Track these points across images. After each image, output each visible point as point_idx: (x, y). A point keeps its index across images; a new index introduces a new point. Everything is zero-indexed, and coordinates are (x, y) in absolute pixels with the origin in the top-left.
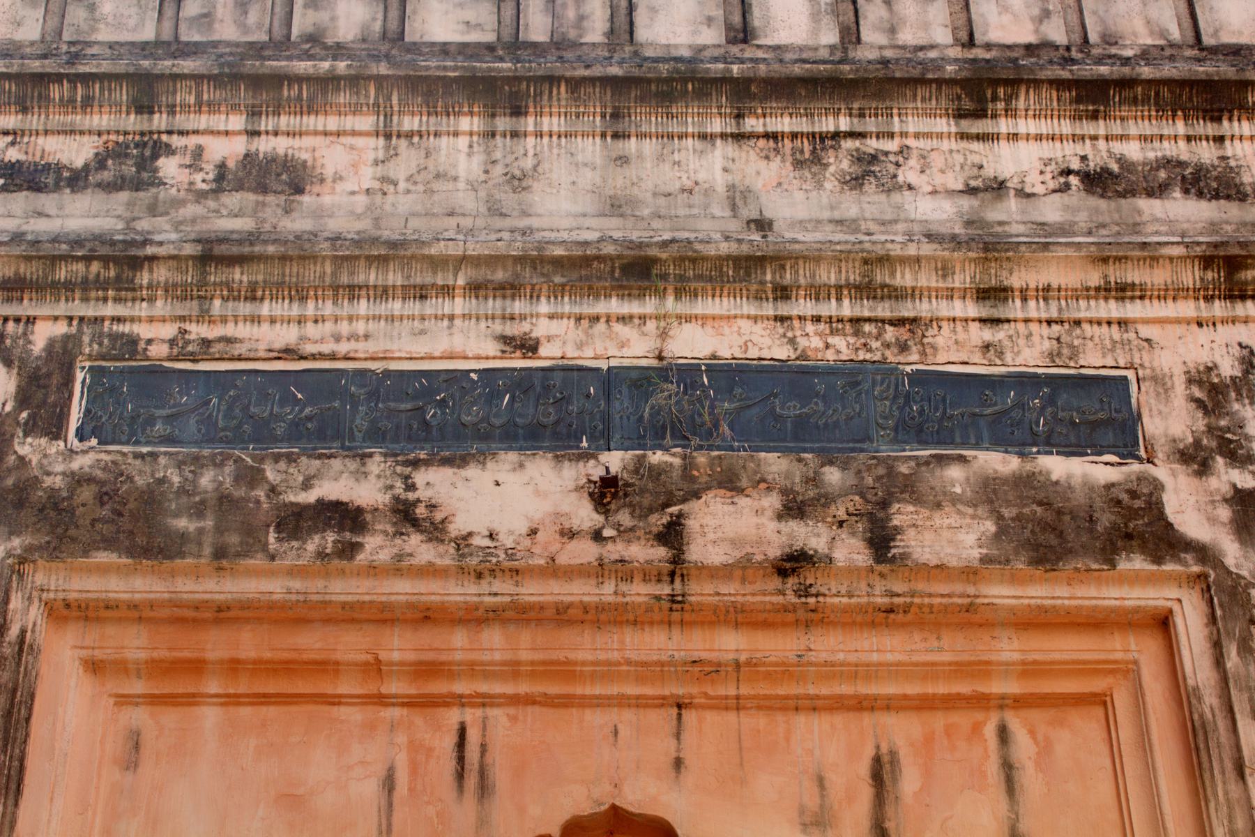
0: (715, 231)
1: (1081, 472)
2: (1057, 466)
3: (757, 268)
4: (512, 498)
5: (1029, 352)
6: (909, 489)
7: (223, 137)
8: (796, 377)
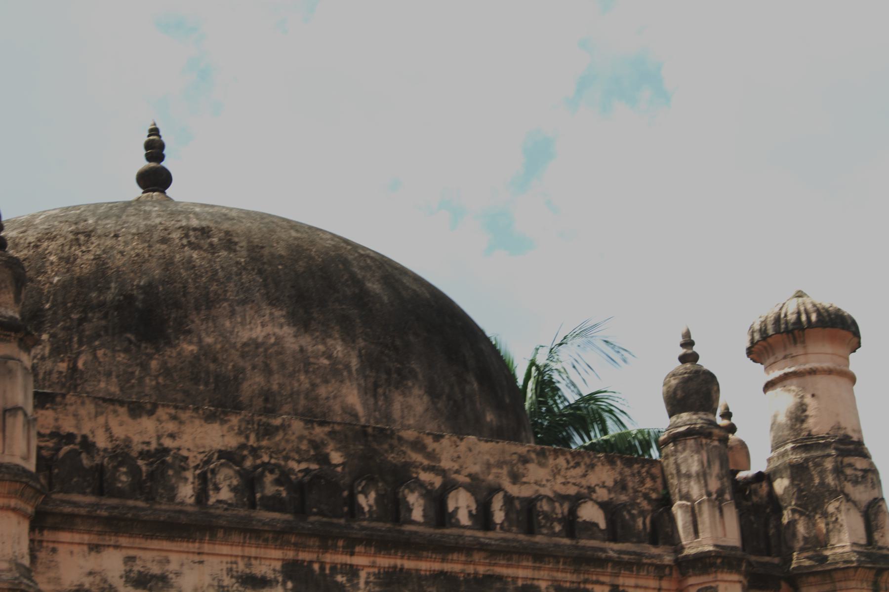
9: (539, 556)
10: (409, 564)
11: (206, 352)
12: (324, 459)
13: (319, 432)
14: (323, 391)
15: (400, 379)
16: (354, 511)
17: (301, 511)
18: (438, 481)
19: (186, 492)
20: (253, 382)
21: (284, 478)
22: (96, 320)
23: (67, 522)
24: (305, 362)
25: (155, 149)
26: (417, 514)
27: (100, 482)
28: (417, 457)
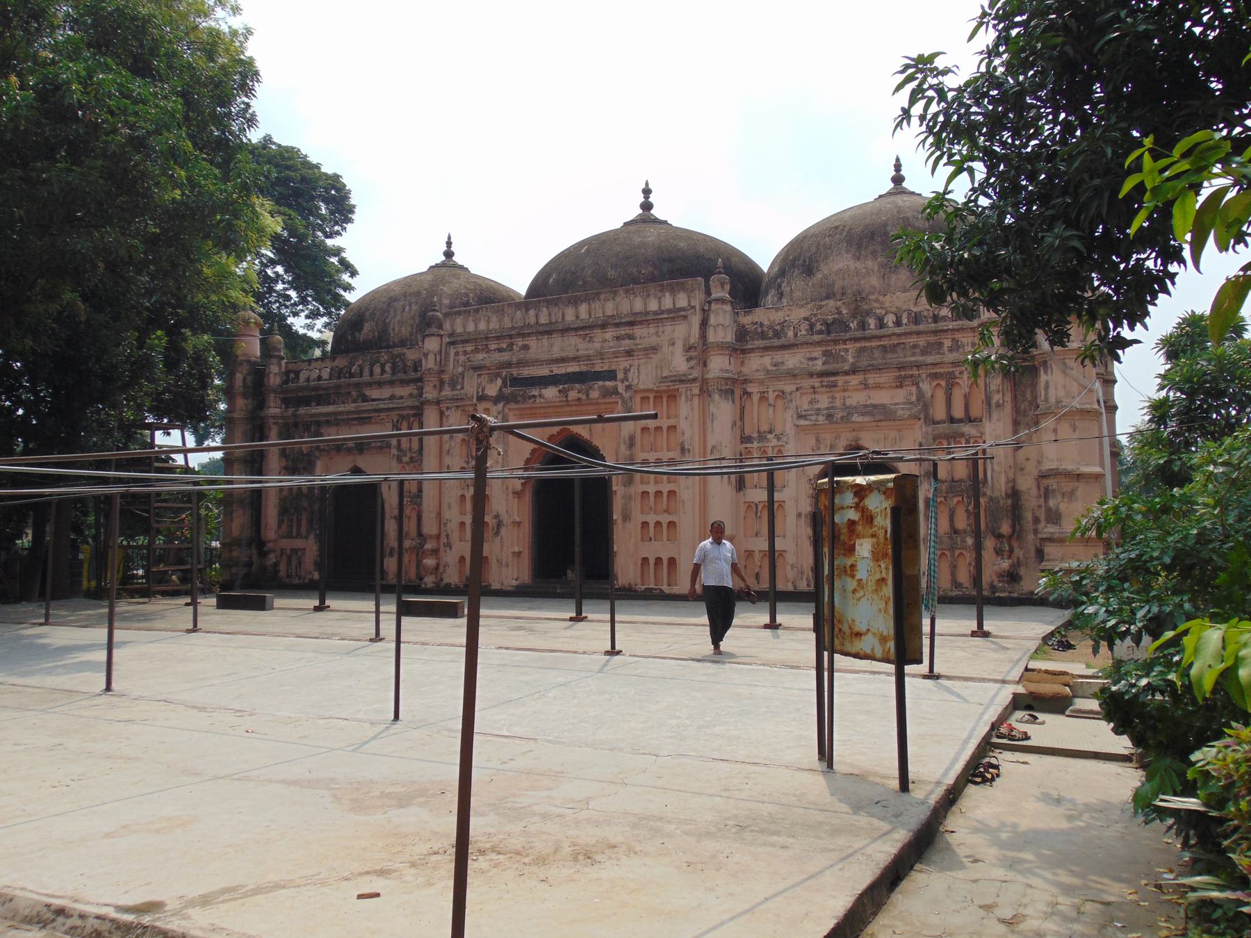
0: (571, 355)
2: (608, 383)
3: (575, 359)
4: (551, 392)
5: (606, 368)
6: (590, 388)
8: (580, 373)
9: (918, 333)
10: (867, 344)
11: (825, 277)
12: (840, 313)
13: (839, 303)
14: (862, 282)
16: (847, 328)
17: (829, 333)
18: (883, 312)
19: (791, 334)
20: (839, 284)
22: (797, 271)
23: (752, 350)
24: (857, 273)
25: (898, 167)
26: (872, 326)
27: (763, 336)
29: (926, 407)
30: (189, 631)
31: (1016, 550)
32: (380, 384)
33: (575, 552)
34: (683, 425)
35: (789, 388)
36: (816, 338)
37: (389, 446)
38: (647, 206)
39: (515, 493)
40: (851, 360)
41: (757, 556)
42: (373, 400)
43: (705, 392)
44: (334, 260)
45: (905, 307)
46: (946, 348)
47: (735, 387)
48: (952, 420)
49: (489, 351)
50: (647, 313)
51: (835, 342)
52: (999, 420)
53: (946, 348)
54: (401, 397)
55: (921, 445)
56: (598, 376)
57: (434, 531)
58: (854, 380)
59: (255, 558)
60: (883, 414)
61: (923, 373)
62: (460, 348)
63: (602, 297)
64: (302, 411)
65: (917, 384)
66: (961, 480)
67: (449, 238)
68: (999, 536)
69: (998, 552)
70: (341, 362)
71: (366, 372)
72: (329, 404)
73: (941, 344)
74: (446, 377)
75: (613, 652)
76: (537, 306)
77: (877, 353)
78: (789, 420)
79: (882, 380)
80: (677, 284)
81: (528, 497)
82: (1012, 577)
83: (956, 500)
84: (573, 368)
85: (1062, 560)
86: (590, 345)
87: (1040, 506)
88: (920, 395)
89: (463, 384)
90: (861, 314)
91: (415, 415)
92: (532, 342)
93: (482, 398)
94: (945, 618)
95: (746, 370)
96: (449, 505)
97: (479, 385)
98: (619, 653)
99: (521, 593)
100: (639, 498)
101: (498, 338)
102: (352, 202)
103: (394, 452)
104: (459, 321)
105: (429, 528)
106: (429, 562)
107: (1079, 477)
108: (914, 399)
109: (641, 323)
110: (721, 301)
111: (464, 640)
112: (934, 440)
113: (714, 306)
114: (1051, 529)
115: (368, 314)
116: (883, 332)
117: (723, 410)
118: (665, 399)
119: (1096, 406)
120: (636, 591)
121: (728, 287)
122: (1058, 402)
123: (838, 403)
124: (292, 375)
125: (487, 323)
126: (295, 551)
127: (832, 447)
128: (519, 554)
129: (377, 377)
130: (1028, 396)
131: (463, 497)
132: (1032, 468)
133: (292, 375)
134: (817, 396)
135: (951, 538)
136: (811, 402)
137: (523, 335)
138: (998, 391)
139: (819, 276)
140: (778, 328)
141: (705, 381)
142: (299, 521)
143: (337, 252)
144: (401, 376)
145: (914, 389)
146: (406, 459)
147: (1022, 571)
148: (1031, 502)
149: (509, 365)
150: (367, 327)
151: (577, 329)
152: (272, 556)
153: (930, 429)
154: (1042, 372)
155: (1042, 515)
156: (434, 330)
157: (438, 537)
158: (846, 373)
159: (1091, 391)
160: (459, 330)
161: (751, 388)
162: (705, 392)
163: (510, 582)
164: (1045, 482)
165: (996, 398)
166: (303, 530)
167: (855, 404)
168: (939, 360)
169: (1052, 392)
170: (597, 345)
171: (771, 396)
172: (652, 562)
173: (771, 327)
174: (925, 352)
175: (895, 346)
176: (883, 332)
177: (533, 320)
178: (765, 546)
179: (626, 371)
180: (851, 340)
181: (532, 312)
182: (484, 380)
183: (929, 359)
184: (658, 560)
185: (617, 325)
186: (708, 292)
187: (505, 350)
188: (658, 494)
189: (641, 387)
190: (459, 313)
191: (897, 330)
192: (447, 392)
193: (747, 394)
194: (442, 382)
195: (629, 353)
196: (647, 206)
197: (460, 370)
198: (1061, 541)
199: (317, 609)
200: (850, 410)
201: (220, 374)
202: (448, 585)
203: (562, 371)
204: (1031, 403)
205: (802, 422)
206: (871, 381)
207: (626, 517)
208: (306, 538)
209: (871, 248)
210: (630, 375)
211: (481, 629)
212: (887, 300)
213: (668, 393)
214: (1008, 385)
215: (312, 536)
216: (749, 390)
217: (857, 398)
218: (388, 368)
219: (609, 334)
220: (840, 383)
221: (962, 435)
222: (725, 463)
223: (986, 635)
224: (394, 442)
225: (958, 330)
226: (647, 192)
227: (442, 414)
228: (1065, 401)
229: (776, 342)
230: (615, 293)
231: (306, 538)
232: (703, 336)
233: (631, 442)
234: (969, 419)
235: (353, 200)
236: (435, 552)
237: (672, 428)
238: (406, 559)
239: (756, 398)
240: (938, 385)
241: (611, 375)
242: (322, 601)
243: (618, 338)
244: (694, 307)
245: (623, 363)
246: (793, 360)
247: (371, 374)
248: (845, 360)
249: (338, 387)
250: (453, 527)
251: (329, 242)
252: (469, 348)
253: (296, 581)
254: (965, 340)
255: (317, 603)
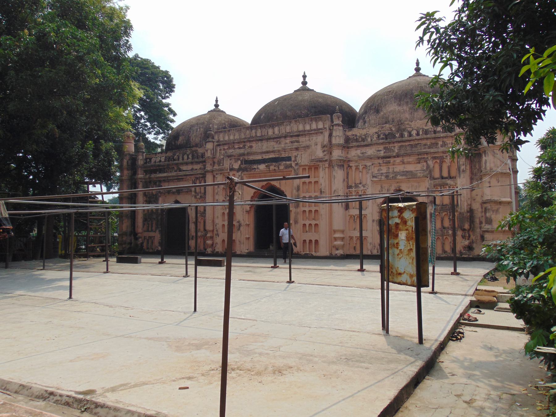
0: (271, 149)
1: (288, 163)
2: (287, 162)
3: (273, 152)
4: (262, 167)
6: (280, 165)
7: (248, 144)
8: (275, 158)
9: (427, 139)
11: (385, 114)
13: (391, 126)
15: (416, 110)
16: (394, 137)
17: (386, 139)
19: (369, 140)
21: (384, 134)
23: (352, 147)
24: (399, 112)
25: (418, 64)
26: (406, 136)
27: (357, 140)
28: (407, 126)
29: (430, 172)
30: (105, 273)
31: (472, 236)
32: (187, 164)
33: (272, 237)
34: (321, 181)
35: (369, 164)
36: (381, 141)
37: (191, 191)
38: (304, 83)
39: (246, 211)
40: (396, 151)
41: (355, 239)
42: (184, 171)
43: (331, 166)
44: (166, 109)
45: (421, 127)
46: (439, 146)
47: (344, 164)
48: (442, 178)
49: (235, 149)
50: (305, 131)
51: (389, 143)
52: (464, 177)
53: (439, 146)
54: (196, 169)
55: (428, 189)
56: (283, 159)
57: (211, 229)
58: (398, 160)
59: (133, 241)
60: (410, 175)
61: (429, 157)
62: (222, 148)
63: (285, 124)
64: (153, 176)
65: (426, 162)
66: (446, 205)
67: (217, 98)
68: (464, 230)
69: (463, 237)
70: (169, 154)
71: (181, 159)
72: (164, 172)
73: (437, 144)
74: (216, 160)
75: (290, 282)
76: (256, 128)
77: (408, 148)
78: (369, 178)
79: (411, 160)
80: (318, 118)
81: (252, 213)
82: (470, 248)
83: (444, 214)
84: (272, 156)
85: (493, 240)
86: (280, 145)
87: (482, 216)
88: (428, 167)
89: (223, 163)
90: (401, 131)
91: (202, 177)
92: (254, 144)
93: (232, 169)
94: (439, 266)
95: (349, 156)
96: (218, 217)
97: (230, 164)
98: (293, 282)
99: (250, 256)
100: (302, 213)
101: (238, 143)
102: (174, 83)
103: (193, 193)
104: (221, 135)
105: (209, 227)
106: (209, 242)
107: (501, 203)
108: (425, 168)
109: (302, 135)
110: (338, 125)
111: (224, 277)
112: (434, 186)
113: (335, 128)
114: (487, 227)
115: (181, 133)
116: (411, 138)
117: (339, 174)
118: (313, 169)
119: (508, 171)
120: (300, 255)
121: (341, 119)
122: (491, 169)
123: (391, 170)
124: (148, 160)
125: (233, 136)
126: (150, 237)
127: (388, 190)
128: (248, 239)
129: (185, 160)
130: (477, 166)
131: (224, 213)
132: (479, 200)
133: (148, 160)
134: (381, 167)
135: (442, 231)
136: (378, 170)
137: (250, 141)
138: (463, 165)
139: (382, 113)
140: (364, 137)
141: (331, 161)
142: (152, 224)
143: (168, 105)
144: (196, 160)
145: (425, 164)
146: (198, 197)
147: (474, 245)
148: (478, 214)
149: (243, 155)
150: (181, 138)
151: (274, 138)
152: (140, 240)
153: (432, 182)
154: (483, 156)
155: (483, 220)
156: (210, 139)
157: (213, 231)
158: (394, 157)
159: (506, 164)
160: (222, 139)
161: (352, 164)
162: (331, 166)
163: (245, 251)
164: (485, 205)
165: (462, 167)
166: (154, 228)
167: (398, 171)
168: (436, 151)
169: (488, 165)
170: (283, 146)
171: (361, 167)
172: (308, 242)
173: (360, 137)
174: (429, 148)
175: (416, 144)
176: (411, 138)
177: (254, 135)
178: (358, 235)
179: (296, 157)
180: (396, 142)
181: (254, 131)
182: (233, 161)
183: (432, 150)
184: (310, 241)
185: (292, 136)
186: (332, 121)
187: (242, 148)
188: (310, 211)
189: (303, 164)
190: (221, 132)
191: (417, 137)
192: (216, 167)
193: (351, 167)
194: (214, 163)
195: (297, 149)
196: (304, 83)
197: (222, 157)
198: (492, 232)
199: (160, 263)
200: (396, 174)
201: (117, 160)
202: (218, 252)
203: (267, 157)
204: (478, 170)
205: (375, 179)
206: (405, 161)
207: (296, 222)
208: (155, 232)
209: (405, 100)
210: (297, 158)
211: (232, 272)
212: (413, 124)
213: (314, 166)
214: (468, 162)
215: (158, 231)
216: (351, 165)
217: (399, 168)
218: (190, 157)
219: (288, 140)
220: (392, 161)
221: (447, 184)
222: (340, 198)
223: (458, 274)
224: (193, 189)
225: (445, 137)
226: (304, 77)
227: (214, 176)
228: (494, 169)
229: (362, 143)
230: (290, 122)
231: (155, 232)
232: (330, 141)
233: (298, 189)
234: (450, 177)
235: (174, 82)
236: (212, 238)
237: (316, 182)
238: (199, 241)
239: (354, 168)
240: (436, 162)
241: (289, 159)
242: (162, 259)
243: (292, 142)
244: (326, 128)
245: (294, 153)
246: (370, 151)
247: (183, 159)
248: (394, 151)
249: (168, 165)
250: (219, 226)
251: (164, 101)
252: (226, 147)
253: (151, 251)
254: (448, 142)
255: (160, 260)
